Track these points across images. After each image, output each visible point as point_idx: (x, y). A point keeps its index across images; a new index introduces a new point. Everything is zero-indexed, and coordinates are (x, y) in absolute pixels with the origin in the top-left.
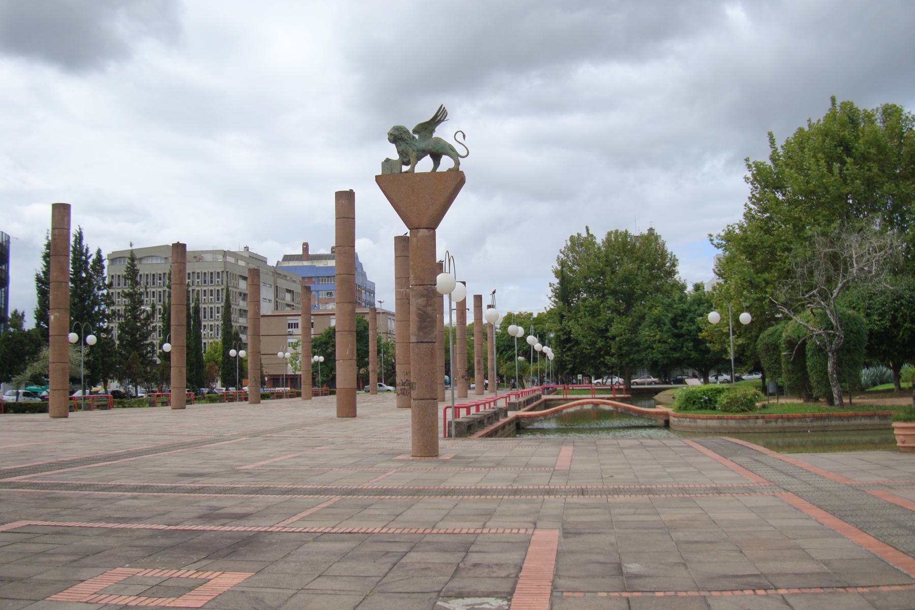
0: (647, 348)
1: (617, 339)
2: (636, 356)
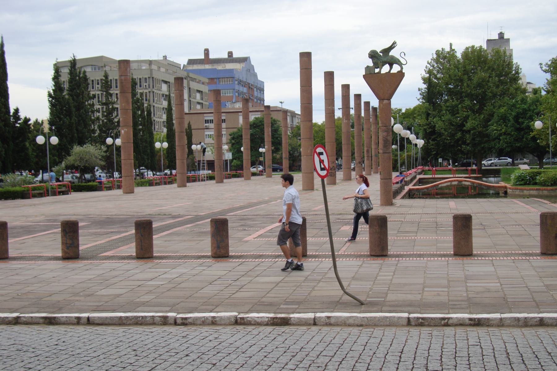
0: (494, 140)
1: (472, 132)
2: (486, 145)
